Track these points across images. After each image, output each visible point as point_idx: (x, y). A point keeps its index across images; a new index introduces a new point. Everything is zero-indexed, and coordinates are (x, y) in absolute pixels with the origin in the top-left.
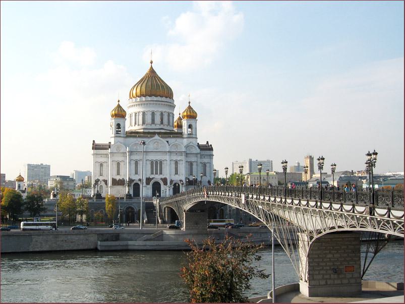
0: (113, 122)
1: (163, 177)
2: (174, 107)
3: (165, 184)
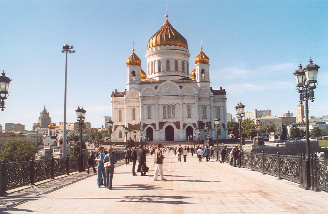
0: (127, 71)
1: (176, 121)
2: (189, 56)
3: (178, 127)
